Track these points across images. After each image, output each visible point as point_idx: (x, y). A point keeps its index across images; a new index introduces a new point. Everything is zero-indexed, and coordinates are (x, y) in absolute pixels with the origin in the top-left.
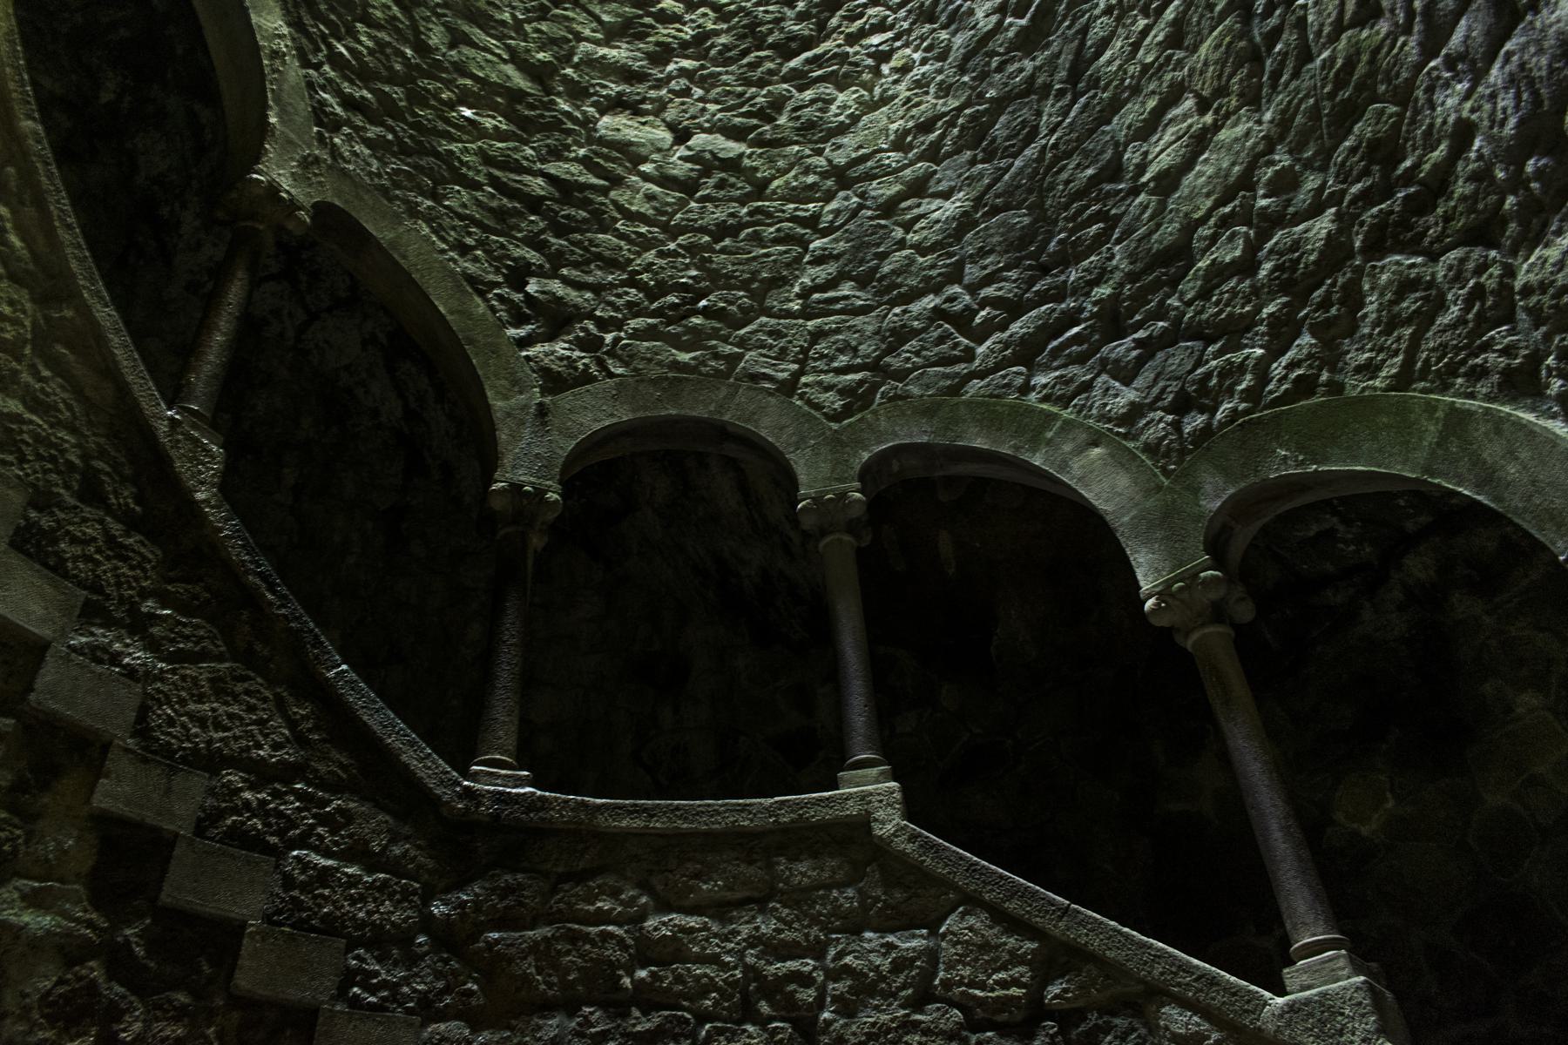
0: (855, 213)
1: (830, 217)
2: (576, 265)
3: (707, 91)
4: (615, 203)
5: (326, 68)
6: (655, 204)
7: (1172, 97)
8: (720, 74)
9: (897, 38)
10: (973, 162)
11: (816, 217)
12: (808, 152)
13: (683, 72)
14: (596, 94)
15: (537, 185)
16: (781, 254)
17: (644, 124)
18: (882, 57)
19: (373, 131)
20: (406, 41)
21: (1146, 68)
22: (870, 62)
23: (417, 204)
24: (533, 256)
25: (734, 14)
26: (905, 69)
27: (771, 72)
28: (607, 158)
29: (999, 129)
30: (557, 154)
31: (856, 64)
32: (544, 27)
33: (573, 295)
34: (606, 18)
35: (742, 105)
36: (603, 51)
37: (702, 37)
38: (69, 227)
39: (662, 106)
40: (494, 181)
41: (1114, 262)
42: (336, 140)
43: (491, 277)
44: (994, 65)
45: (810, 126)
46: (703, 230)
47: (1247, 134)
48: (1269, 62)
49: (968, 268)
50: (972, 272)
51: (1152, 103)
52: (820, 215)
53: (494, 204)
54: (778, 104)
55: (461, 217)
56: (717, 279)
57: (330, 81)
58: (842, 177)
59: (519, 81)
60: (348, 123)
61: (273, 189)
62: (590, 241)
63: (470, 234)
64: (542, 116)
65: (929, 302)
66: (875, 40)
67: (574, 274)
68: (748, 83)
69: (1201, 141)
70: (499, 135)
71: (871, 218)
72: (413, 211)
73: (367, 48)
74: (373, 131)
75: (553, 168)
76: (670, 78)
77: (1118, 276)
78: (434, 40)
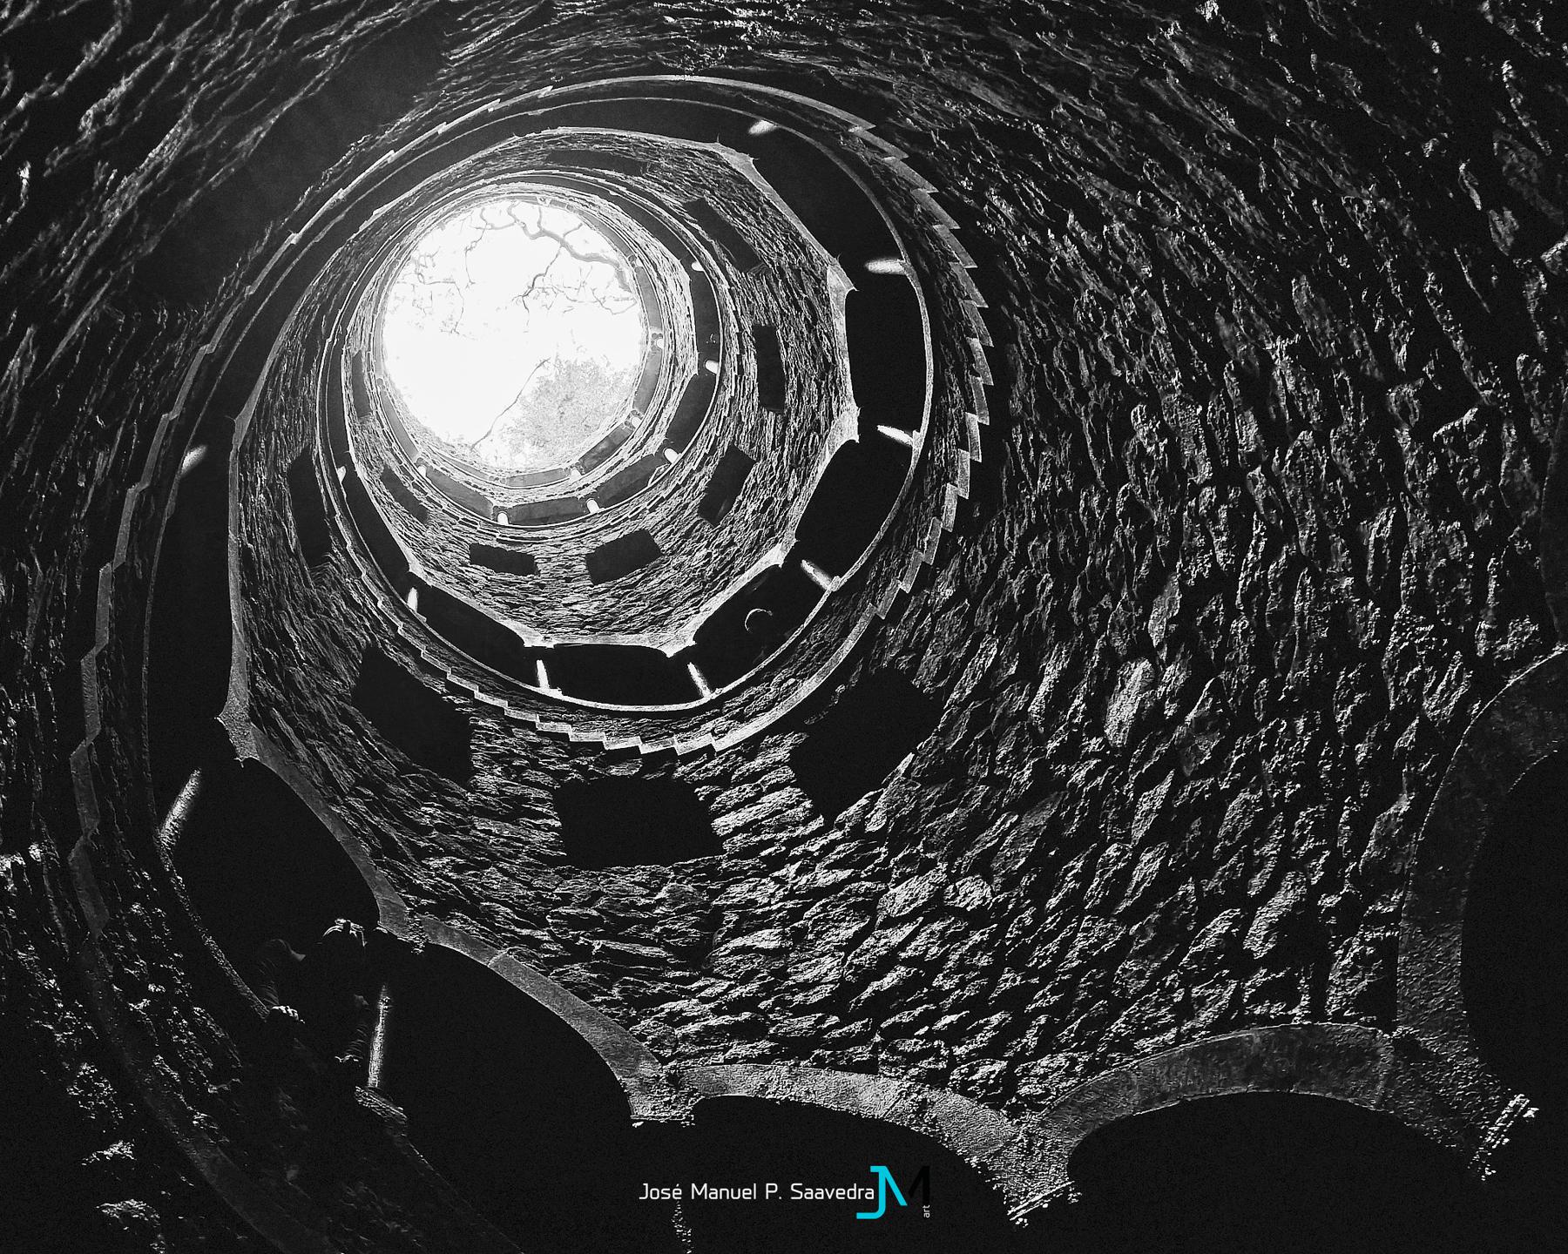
0: (1272, 480)
2: (1250, 872)
3: (1107, 589)
8: (1092, 565)
11: (1271, 531)
12: (1193, 503)
13: (1083, 608)
15: (1149, 865)
16: (1304, 599)
17: (1123, 687)
20: (965, 935)
22: (1107, 386)
23: (1118, 1035)
24: (1219, 926)
25: (1039, 515)
27: (1101, 505)
28: (1145, 757)
30: (1126, 815)
31: (1107, 402)
34: (1012, 670)
36: (1043, 689)
37: (1053, 563)
39: (1108, 651)
40: (1127, 918)
43: (1227, 995)
45: (1164, 485)
46: (1253, 681)
54: (1135, 511)
55: (1150, 988)
56: (1316, 696)
58: (1229, 475)
62: (1225, 837)
63: (1172, 989)
64: (1083, 810)
65: (1404, 437)
66: (1085, 372)
68: (1106, 538)
70: (1085, 878)
71: (1282, 464)
72: (1124, 1045)
73: (958, 986)
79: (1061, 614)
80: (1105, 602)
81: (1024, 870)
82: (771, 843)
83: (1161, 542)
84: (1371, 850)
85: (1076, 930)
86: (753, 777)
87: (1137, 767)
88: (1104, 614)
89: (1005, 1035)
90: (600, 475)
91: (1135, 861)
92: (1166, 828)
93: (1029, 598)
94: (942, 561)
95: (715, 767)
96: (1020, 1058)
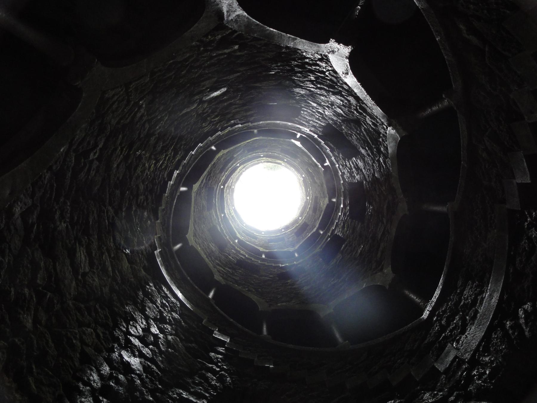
0: (140, 134)
5: (325, 70)
7: (91, 264)
9: (156, 169)
10: (118, 178)
18: (157, 161)
19: (307, 60)
21: (102, 253)
26: (150, 167)
29: (118, 192)
33: (220, 52)
41: (63, 223)
44: (131, 197)
47: (70, 294)
48: (82, 306)
49: (98, 163)
50: (96, 164)
51: (94, 252)
53: (257, 59)
60: (316, 61)
67: (222, 57)
69: (75, 271)
74: (307, 60)
76: (209, 109)
77: (58, 223)
78: (288, 82)
79: (213, 112)
80: (200, 112)
83: (176, 123)
84: (188, 55)
86: (307, 122)
88: (203, 110)
90: (279, 161)
93: (217, 116)
94: (227, 127)
95: (312, 129)
96: (312, 60)
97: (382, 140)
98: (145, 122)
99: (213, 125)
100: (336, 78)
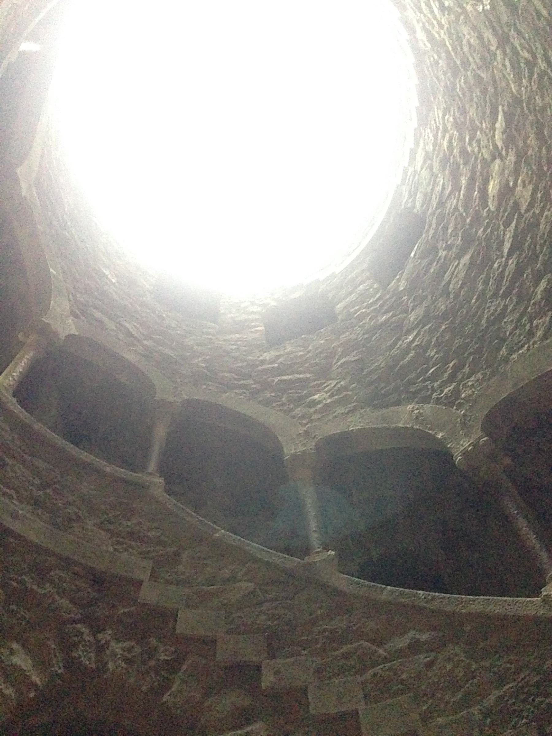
1: (525, 51)
4: (527, 211)
6: (527, 182)
11: (527, 62)
13: (470, 144)
14: (478, 205)
32: (450, 231)
35: (481, 105)
38: (433, 599)
40: (505, 296)
42: (463, 396)
45: (483, 58)
46: (540, 151)
52: (526, 59)
53: (515, 300)
55: (516, 328)
57: (440, 386)
59: (466, 259)
61: (465, 454)
63: (525, 325)
68: (471, 100)
70: (486, 282)
72: (506, 360)
73: (437, 353)
74: (466, 369)
75: (506, 251)
81: (461, 288)
82: (359, 310)
85: (484, 309)
87: (503, 216)
89: (457, 369)
91: (506, 265)
92: (516, 246)
94: (417, 143)
97: (283, 404)
98: (534, 57)
99: (438, 128)
100: (415, 393)
